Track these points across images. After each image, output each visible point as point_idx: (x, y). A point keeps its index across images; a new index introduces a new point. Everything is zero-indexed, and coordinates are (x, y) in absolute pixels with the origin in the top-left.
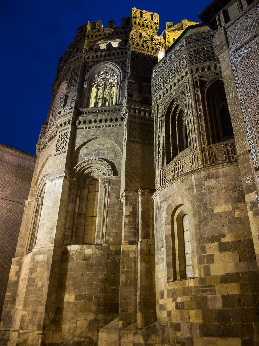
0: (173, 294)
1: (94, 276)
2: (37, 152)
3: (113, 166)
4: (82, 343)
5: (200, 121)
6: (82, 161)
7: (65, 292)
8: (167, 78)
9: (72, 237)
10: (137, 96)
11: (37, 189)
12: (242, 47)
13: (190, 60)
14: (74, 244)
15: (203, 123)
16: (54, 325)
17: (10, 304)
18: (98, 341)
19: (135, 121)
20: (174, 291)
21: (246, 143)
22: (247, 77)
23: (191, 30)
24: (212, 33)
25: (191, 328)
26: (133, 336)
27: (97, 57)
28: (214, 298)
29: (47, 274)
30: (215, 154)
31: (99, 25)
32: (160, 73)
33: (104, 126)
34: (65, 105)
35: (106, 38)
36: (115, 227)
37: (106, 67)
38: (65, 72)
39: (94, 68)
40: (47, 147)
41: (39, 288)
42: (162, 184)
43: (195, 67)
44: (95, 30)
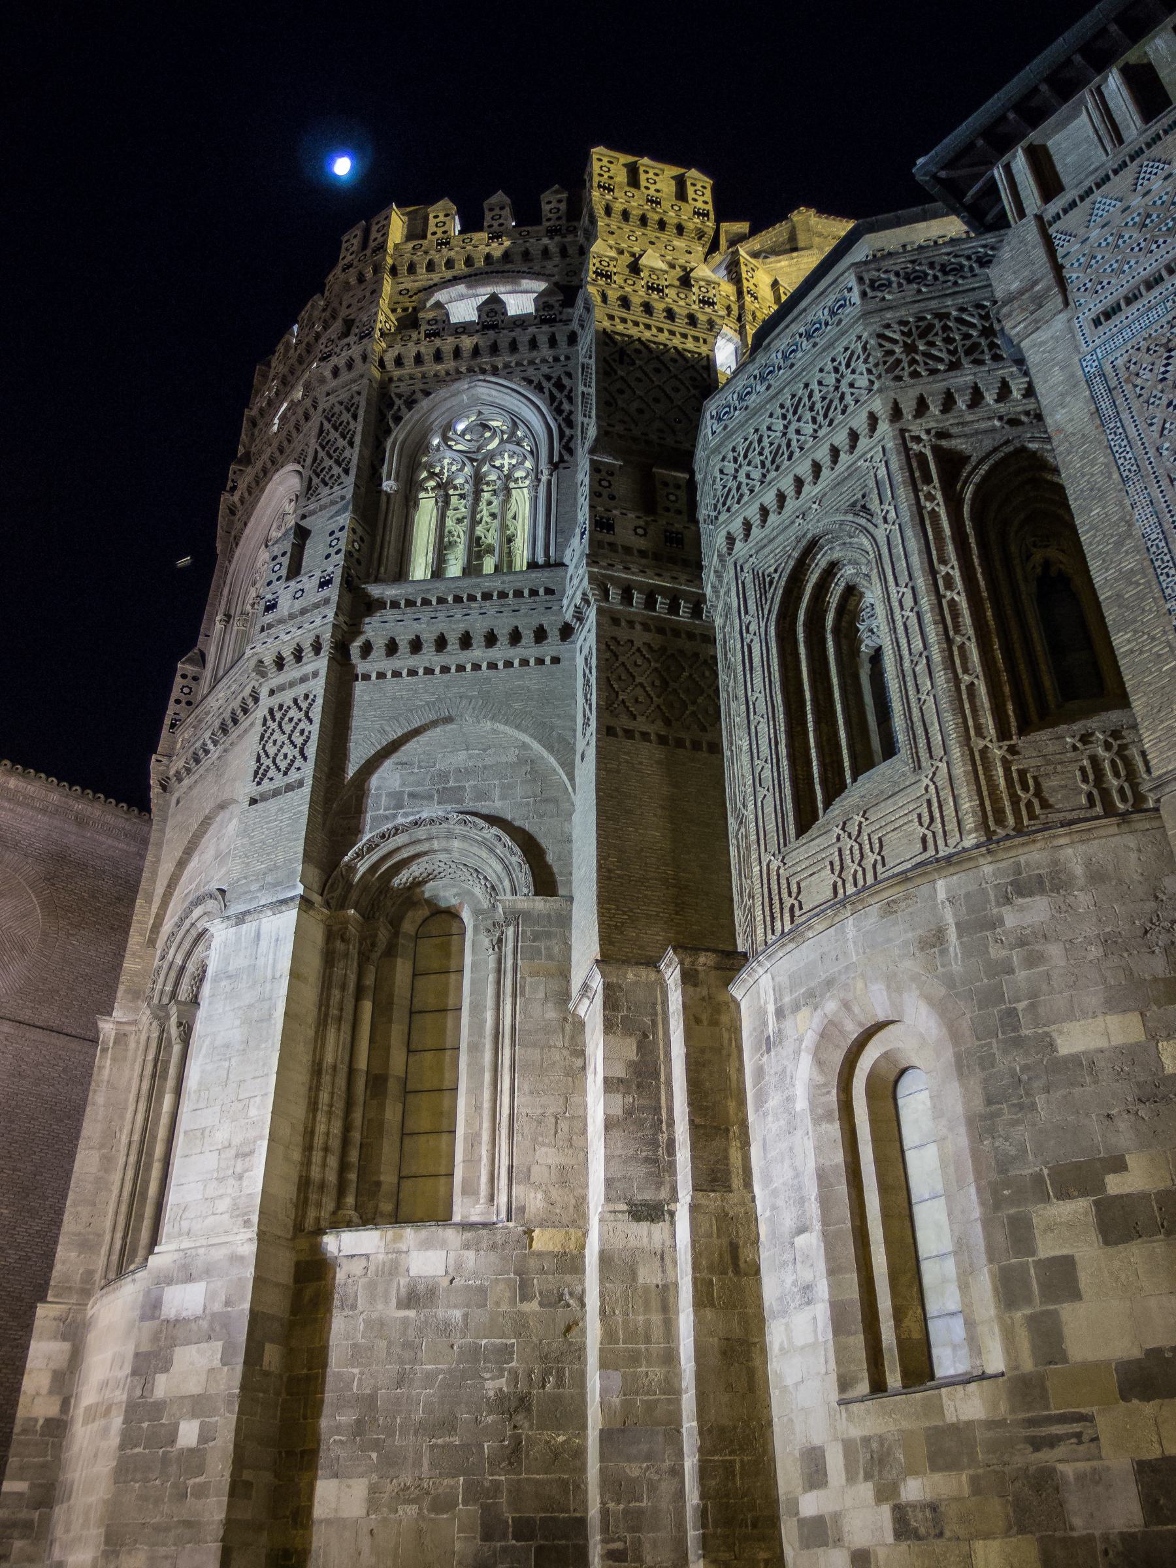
2: (155, 790)
5: (951, 633)
6: (384, 828)
7: (317, 1469)
8: (779, 446)
10: (636, 528)
12: (1129, 301)
13: (885, 363)
14: (349, 1225)
15: (969, 639)
19: (632, 642)
22: (1170, 431)
23: (868, 237)
24: (977, 245)
27: (438, 357)
28: (1096, 1478)
30: (1035, 778)
31: (441, 218)
32: (742, 425)
33: (484, 666)
34: (295, 570)
35: (476, 275)
36: (551, 1137)
37: (476, 401)
38: (290, 426)
39: (425, 404)
40: (206, 762)
42: (783, 925)
43: (913, 394)
44: (425, 243)
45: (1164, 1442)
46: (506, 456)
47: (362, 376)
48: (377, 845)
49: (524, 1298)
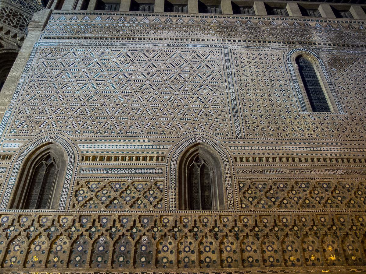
12: (53, 38)
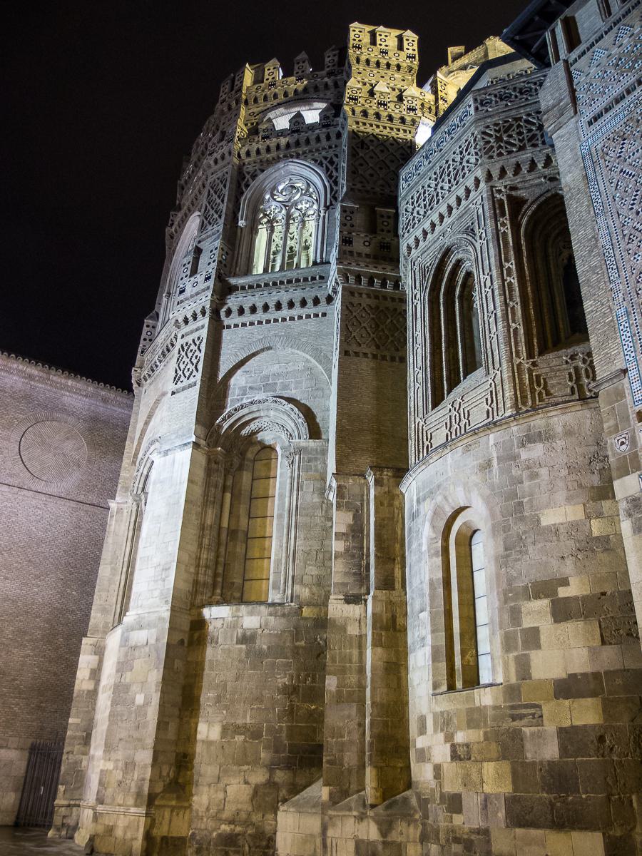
0: (445, 723)
1: (265, 681)
2: (135, 385)
3: (309, 415)
4: (240, 837)
5: (508, 300)
8: (433, 196)
9: (214, 585)
11: (135, 474)
12: (607, 110)
13: (485, 148)
14: (218, 604)
15: (517, 303)
16: (175, 796)
17: (79, 744)
18: (275, 834)
19: (360, 304)
20: (448, 715)
21: (616, 351)
25: (486, 806)
26: (355, 822)
27: (268, 150)
28: (540, 735)
29: (155, 676)
30: (544, 379)
32: (416, 183)
34: (194, 271)
38: (196, 191)
39: (261, 176)
40: (156, 373)
41: (139, 706)
43: (498, 166)
44: (263, 85)
45: (573, 718)
46: (304, 203)
47: (229, 163)
48: (233, 414)
49: (297, 641)
